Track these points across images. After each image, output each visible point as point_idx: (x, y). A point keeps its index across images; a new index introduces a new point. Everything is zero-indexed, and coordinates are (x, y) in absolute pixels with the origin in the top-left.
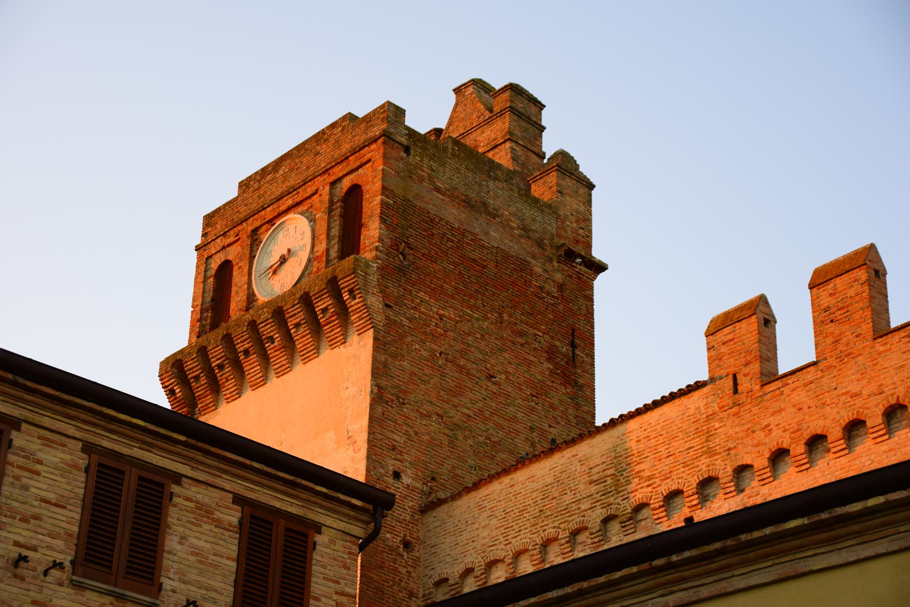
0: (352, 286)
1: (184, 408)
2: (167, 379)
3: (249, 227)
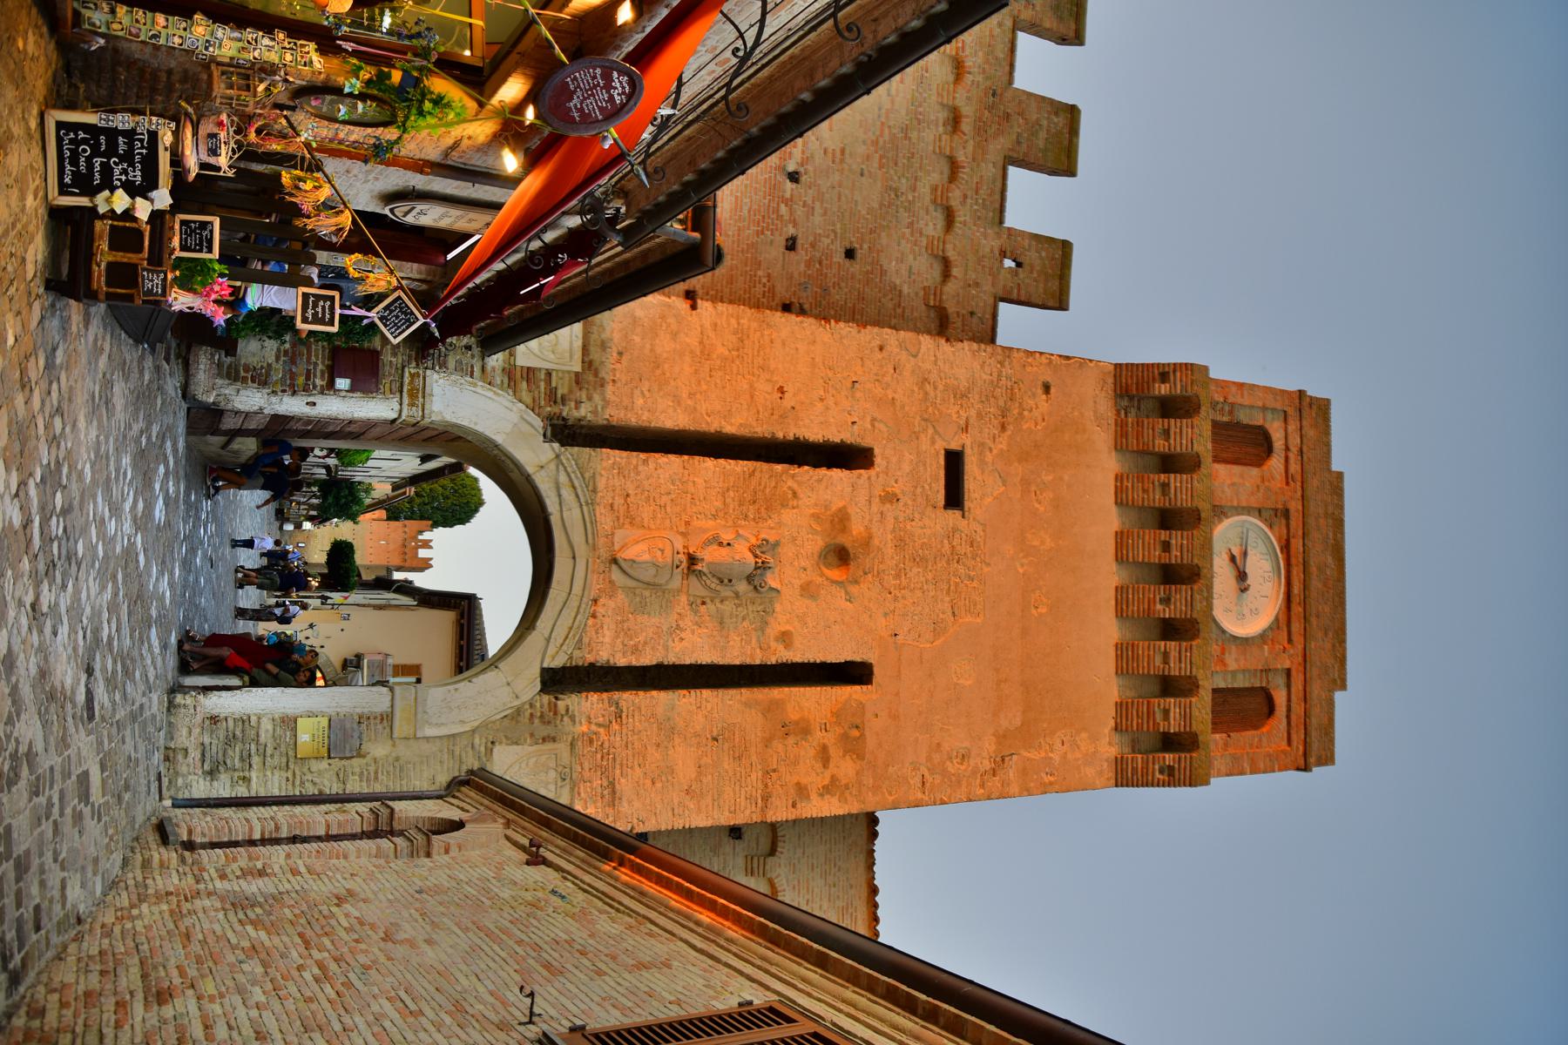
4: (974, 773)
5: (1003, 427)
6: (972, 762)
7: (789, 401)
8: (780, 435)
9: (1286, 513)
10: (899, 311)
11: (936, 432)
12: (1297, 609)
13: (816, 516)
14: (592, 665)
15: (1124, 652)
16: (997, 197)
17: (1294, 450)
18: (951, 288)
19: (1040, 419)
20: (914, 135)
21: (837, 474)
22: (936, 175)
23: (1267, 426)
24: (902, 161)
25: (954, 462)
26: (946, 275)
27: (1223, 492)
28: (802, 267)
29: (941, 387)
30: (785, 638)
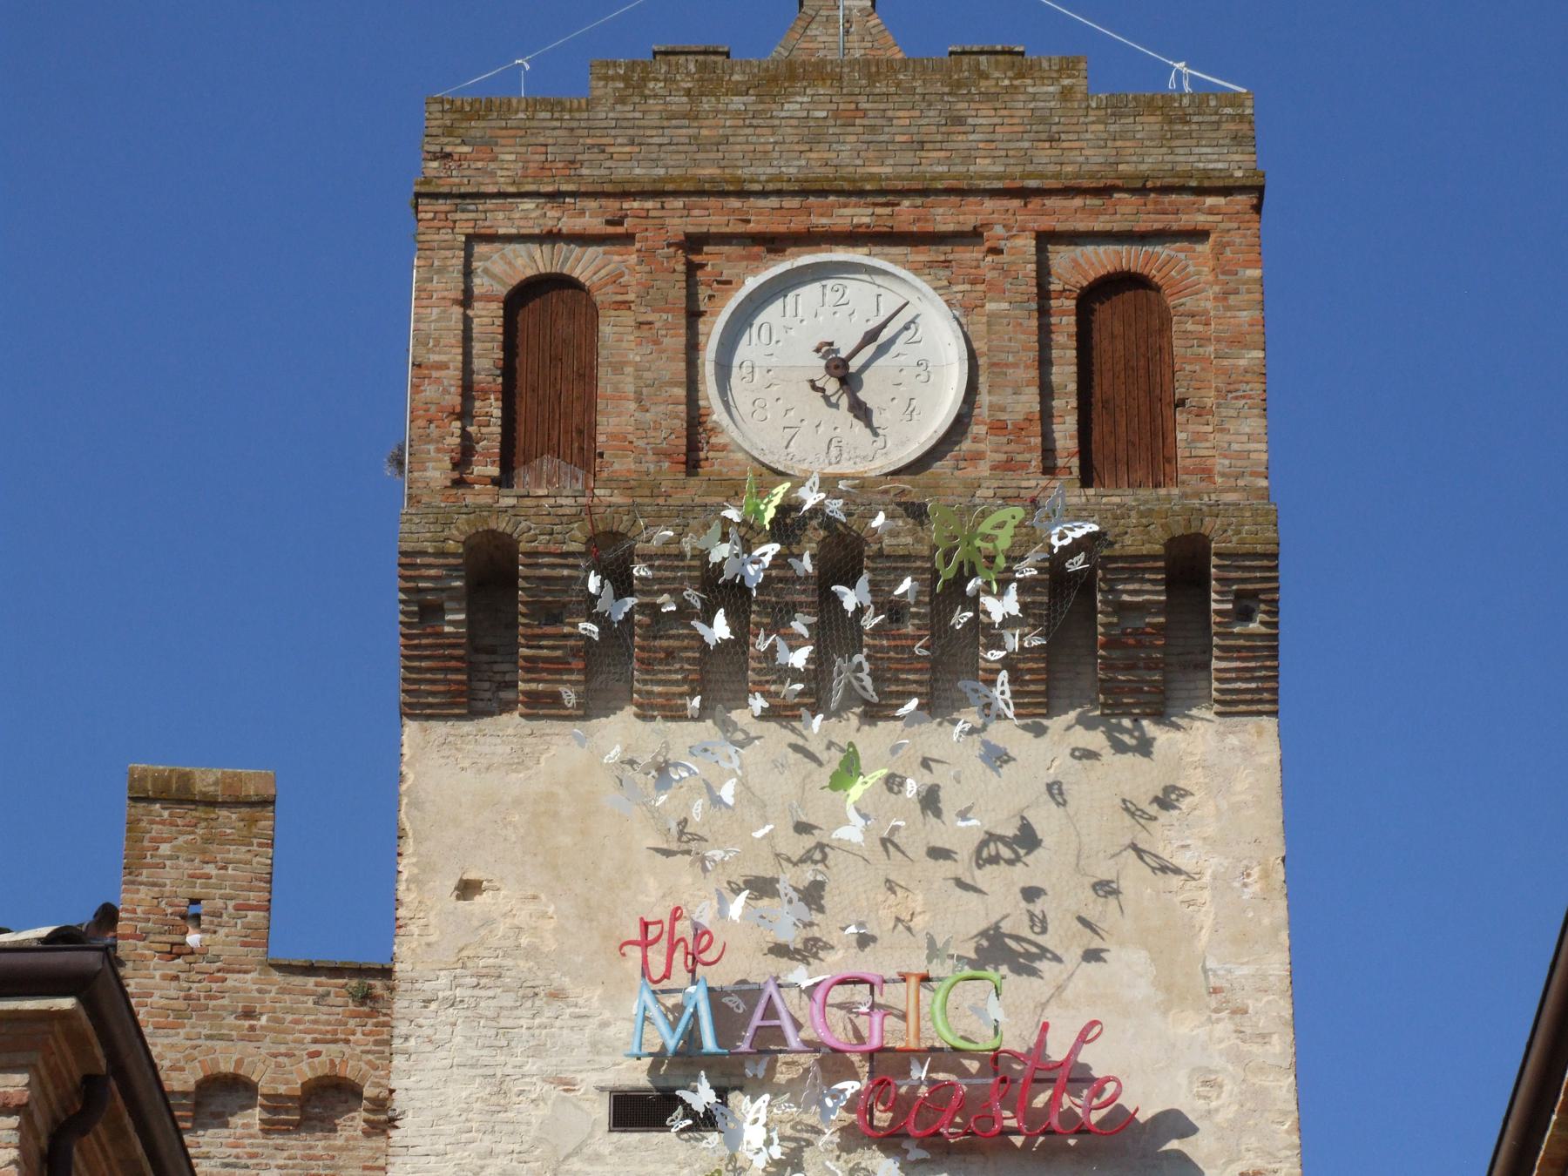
0: (1258, 586)
1: (457, 670)
2: (432, 572)
3: (680, 219)
4: (1238, 1058)
5: (557, 995)
6: (1218, 1062)
9: (693, 243)
11: (576, 1152)
12: (905, 215)
18: (266, 1080)
19: (532, 907)
23: (502, 291)
27: (657, 426)
29: (487, 1142)
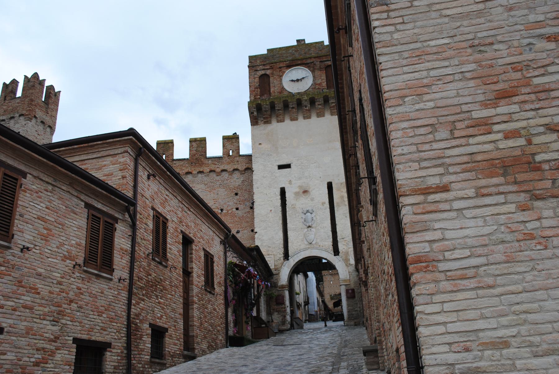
7: (273, 209)
8: (281, 210)
10: (247, 180)
12: (305, 61)
13: (296, 200)
14: (333, 245)
15: (320, 115)
16: (216, 159)
17: (264, 67)
18: (240, 168)
20: (206, 182)
21: (287, 195)
22: (213, 175)
23: (258, 76)
24: (213, 184)
25: (281, 167)
26: (237, 170)
28: (242, 206)
30: (323, 204)
